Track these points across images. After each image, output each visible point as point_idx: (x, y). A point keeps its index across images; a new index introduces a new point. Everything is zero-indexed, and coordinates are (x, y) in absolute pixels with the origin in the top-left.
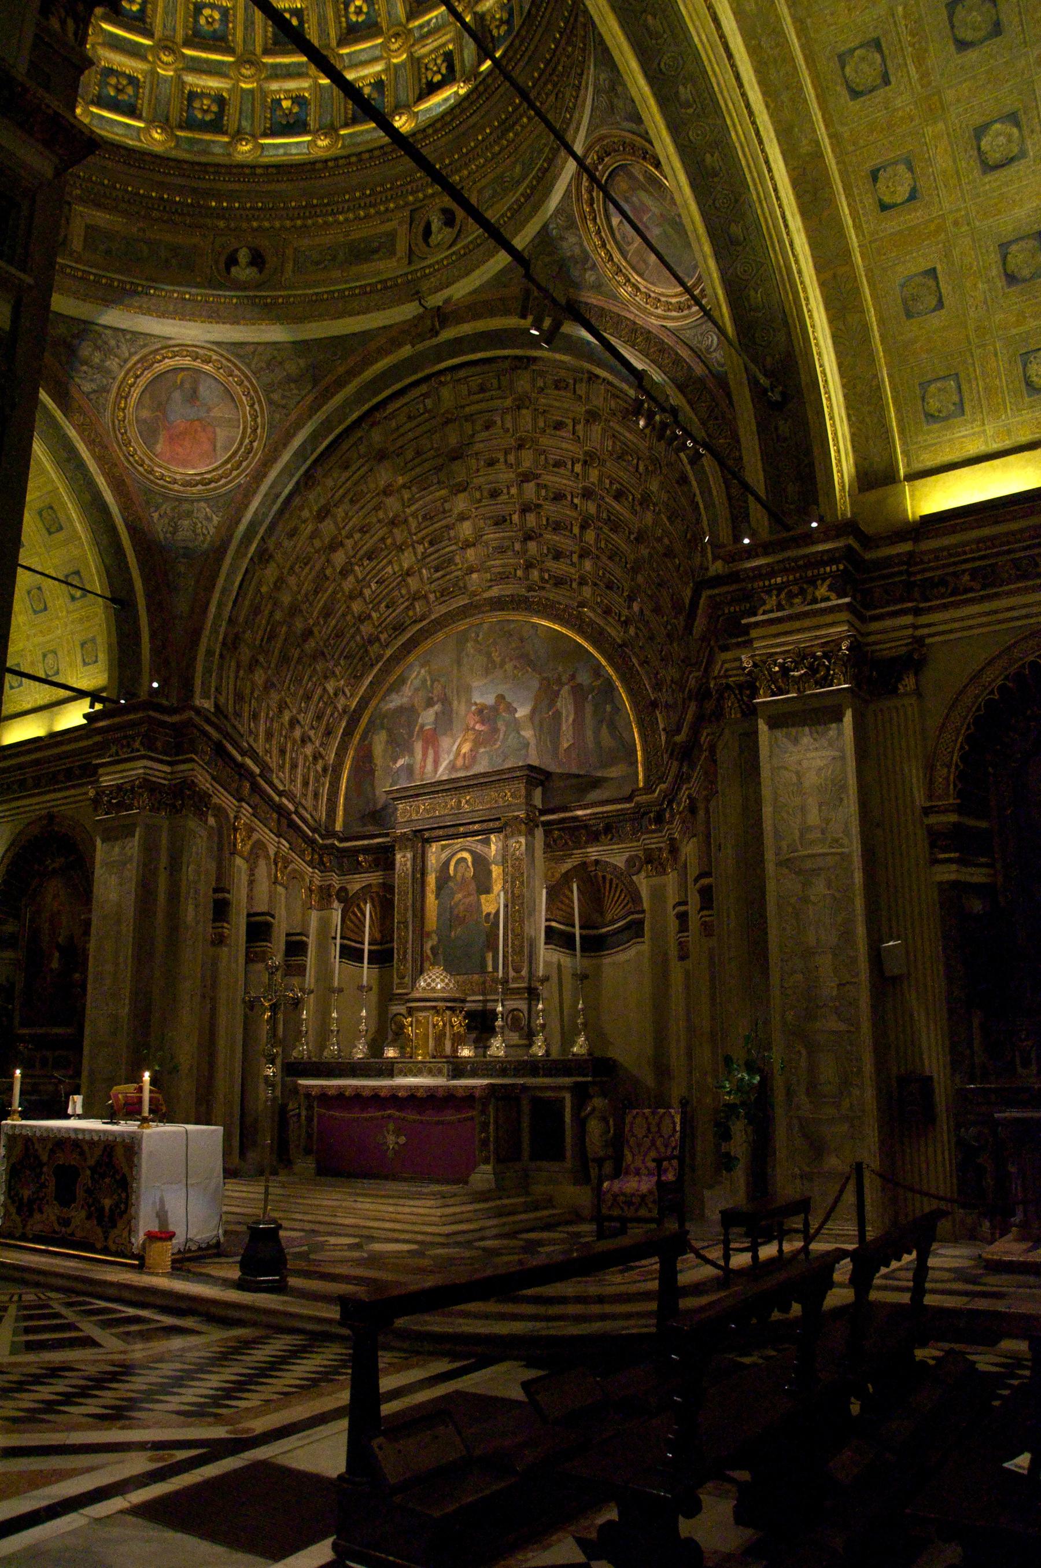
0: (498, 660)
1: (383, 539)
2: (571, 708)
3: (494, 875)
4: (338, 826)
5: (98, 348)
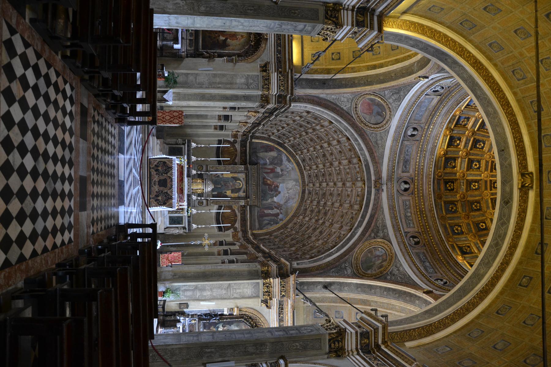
0: (289, 192)
1: (327, 159)
2: (274, 213)
3: (236, 194)
4: (253, 140)
5: (396, 99)
